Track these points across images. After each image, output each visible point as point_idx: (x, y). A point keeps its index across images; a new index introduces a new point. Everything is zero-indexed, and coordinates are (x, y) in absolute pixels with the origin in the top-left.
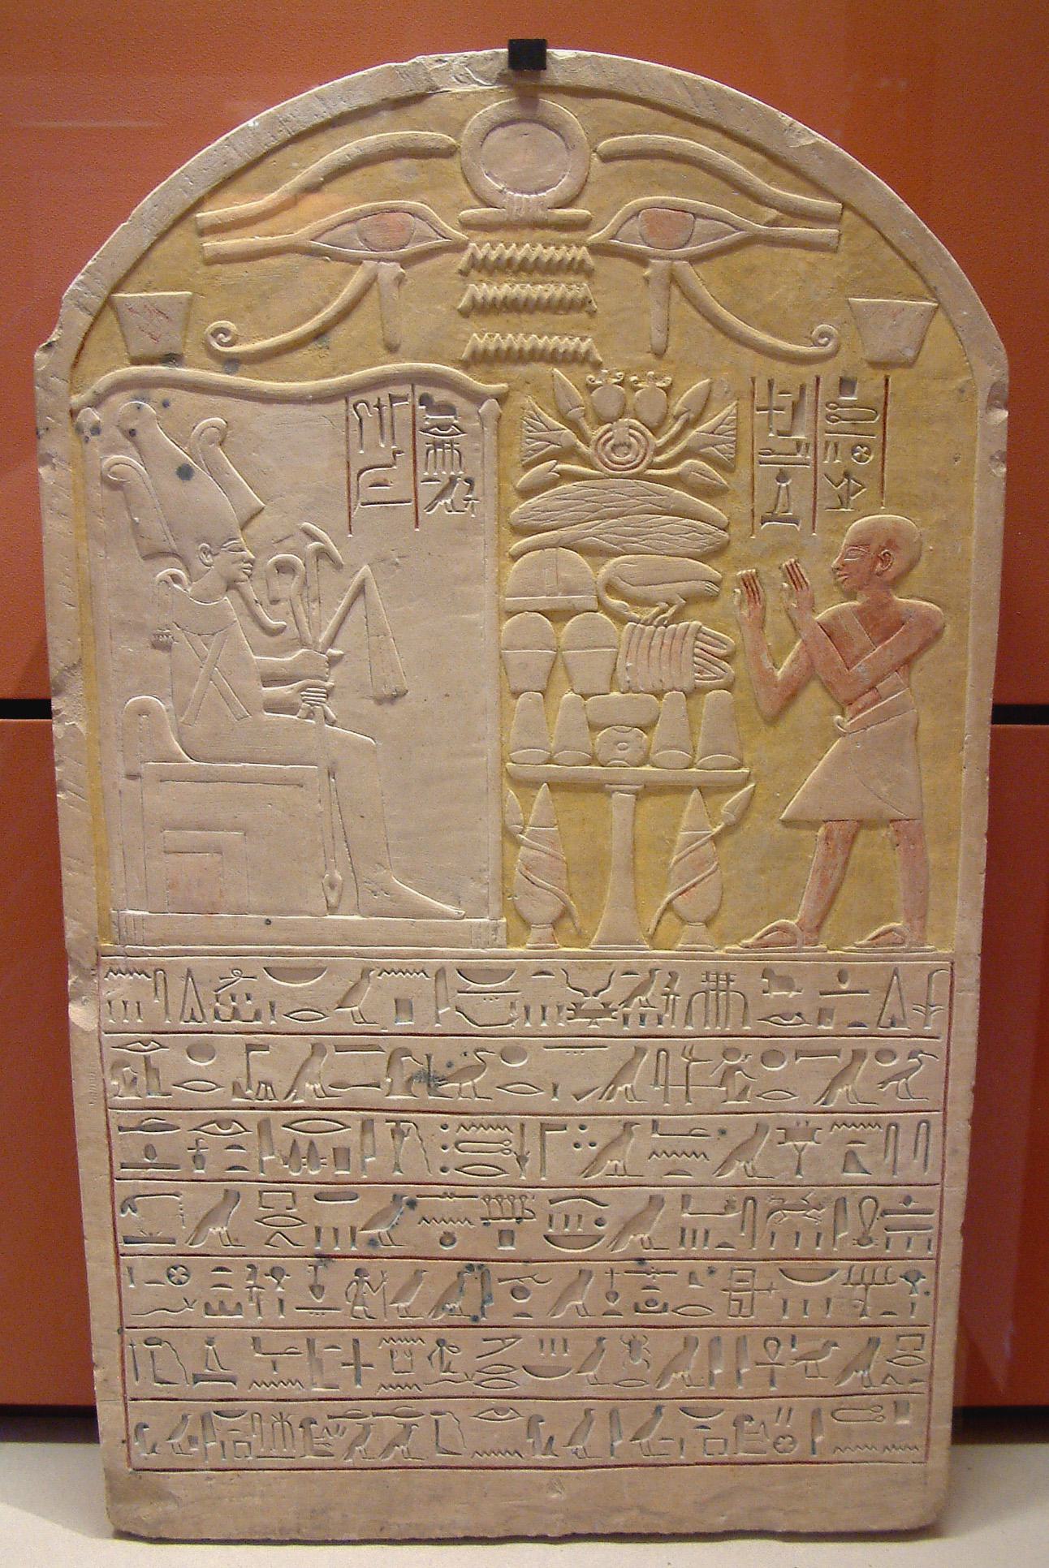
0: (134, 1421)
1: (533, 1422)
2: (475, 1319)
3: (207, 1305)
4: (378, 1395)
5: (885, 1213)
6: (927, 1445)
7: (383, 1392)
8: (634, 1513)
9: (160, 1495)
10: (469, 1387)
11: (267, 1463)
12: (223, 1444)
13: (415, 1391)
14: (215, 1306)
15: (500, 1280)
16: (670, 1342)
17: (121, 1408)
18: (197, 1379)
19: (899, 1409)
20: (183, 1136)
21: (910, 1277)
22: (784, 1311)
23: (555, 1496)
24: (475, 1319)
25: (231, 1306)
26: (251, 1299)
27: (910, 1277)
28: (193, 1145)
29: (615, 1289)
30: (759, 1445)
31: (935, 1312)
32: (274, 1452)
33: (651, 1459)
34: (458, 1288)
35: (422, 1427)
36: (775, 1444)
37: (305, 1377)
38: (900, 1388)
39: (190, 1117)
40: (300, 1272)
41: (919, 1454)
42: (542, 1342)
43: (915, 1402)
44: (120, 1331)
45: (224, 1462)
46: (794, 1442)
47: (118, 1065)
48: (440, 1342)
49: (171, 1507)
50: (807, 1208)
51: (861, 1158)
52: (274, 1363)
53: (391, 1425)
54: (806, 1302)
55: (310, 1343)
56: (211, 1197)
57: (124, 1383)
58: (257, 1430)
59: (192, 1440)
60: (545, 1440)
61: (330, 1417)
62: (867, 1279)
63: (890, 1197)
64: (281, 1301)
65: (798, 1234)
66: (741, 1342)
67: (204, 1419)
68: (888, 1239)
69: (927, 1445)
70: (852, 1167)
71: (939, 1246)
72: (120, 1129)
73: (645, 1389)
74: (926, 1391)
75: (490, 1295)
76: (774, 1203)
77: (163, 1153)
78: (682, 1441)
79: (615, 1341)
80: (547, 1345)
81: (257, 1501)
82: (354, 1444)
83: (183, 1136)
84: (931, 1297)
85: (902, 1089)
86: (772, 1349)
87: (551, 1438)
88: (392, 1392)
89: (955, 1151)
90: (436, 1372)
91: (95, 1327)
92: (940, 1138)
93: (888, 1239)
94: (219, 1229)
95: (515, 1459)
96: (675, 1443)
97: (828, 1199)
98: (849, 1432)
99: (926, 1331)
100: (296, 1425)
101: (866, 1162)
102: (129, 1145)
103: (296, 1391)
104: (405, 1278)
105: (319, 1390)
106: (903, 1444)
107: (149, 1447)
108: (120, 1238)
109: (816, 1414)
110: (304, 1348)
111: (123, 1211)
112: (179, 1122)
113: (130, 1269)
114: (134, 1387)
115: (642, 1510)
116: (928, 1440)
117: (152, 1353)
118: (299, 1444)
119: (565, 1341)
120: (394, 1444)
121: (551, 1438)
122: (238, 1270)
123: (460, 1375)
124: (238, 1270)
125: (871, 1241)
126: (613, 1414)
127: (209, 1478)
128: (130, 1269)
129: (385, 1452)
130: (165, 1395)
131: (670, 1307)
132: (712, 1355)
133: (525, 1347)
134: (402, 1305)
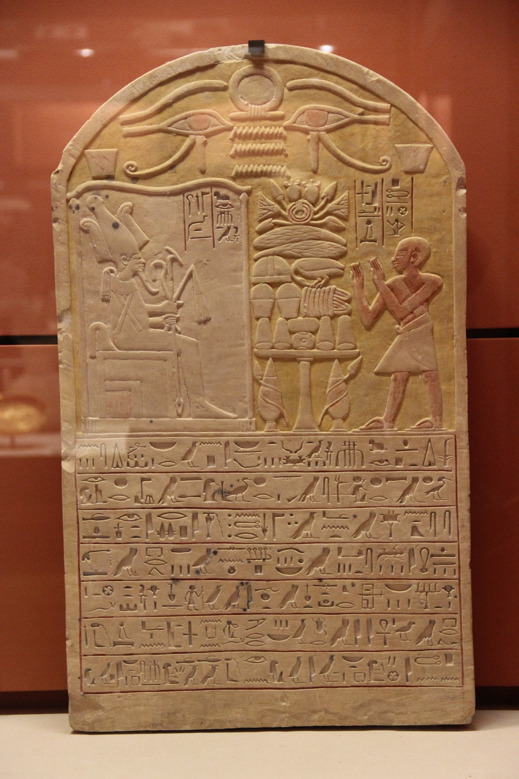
0: (84, 667)
1: (273, 664)
2: (245, 610)
3: (121, 606)
4: (200, 650)
5: (432, 556)
6: (463, 677)
7: (202, 649)
8: (323, 713)
9: (96, 707)
10: (242, 645)
11: (147, 688)
12: (126, 678)
13: (217, 648)
14: (125, 607)
15: (256, 590)
16: (335, 622)
17: (79, 661)
18: (115, 644)
19: (448, 658)
20: (112, 522)
21: (448, 588)
23: (284, 704)
24: (245, 610)
25: (132, 606)
26: (141, 602)
27: (448, 588)
28: (116, 526)
29: (309, 595)
30: (381, 676)
31: (460, 606)
32: (151, 682)
33: (329, 684)
34: (236, 595)
35: (221, 666)
36: (389, 676)
37: (165, 642)
38: (446, 646)
40: (164, 588)
41: (459, 682)
42: (276, 622)
43: (455, 654)
44: (80, 620)
45: (127, 688)
46: (397, 675)
48: (229, 623)
49: (101, 713)
50: (396, 553)
51: (420, 529)
52: (152, 635)
54: (398, 601)
55: (169, 624)
56: (124, 552)
58: (143, 669)
59: (112, 677)
60: (279, 674)
61: (178, 663)
62: (427, 589)
63: (435, 548)
64: (155, 603)
65: (392, 567)
66: (369, 622)
68: (435, 569)
69: (463, 677)
70: (416, 533)
73: (326, 646)
74: (460, 648)
75: (251, 598)
76: (380, 551)
78: (344, 674)
79: (310, 621)
81: (142, 708)
83: (112, 522)
84: (458, 598)
85: (436, 496)
86: (384, 625)
88: (207, 649)
89: (463, 526)
90: (226, 637)
91: (68, 618)
92: (456, 519)
93: (435, 569)
94: (127, 567)
95: (264, 684)
96: (340, 675)
97: (405, 549)
98: (424, 670)
99: (457, 616)
100: (161, 667)
101: (421, 530)
103: (162, 649)
104: (212, 590)
105: (172, 648)
106: (451, 676)
107: (91, 681)
108: (81, 573)
109: (407, 661)
110: (165, 627)
111: (83, 560)
112: (110, 515)
113: (86, 589)
114: (86, 648)
115: (327, 711)
116: (463, 674)
117: (94, 632)
118: (162, 677)
119: (287, 622)
120: (207, 677)
122: (135, 589)
123: (238, 639)
124: (135, 589)
125: (427, 571)
126: (311, 660)
127: (119, 697)
128: (86, 589)
129: (203, 681)
131: (335, 604)
132: (356, 630)
133: (268, 624)
134: (211, 603)
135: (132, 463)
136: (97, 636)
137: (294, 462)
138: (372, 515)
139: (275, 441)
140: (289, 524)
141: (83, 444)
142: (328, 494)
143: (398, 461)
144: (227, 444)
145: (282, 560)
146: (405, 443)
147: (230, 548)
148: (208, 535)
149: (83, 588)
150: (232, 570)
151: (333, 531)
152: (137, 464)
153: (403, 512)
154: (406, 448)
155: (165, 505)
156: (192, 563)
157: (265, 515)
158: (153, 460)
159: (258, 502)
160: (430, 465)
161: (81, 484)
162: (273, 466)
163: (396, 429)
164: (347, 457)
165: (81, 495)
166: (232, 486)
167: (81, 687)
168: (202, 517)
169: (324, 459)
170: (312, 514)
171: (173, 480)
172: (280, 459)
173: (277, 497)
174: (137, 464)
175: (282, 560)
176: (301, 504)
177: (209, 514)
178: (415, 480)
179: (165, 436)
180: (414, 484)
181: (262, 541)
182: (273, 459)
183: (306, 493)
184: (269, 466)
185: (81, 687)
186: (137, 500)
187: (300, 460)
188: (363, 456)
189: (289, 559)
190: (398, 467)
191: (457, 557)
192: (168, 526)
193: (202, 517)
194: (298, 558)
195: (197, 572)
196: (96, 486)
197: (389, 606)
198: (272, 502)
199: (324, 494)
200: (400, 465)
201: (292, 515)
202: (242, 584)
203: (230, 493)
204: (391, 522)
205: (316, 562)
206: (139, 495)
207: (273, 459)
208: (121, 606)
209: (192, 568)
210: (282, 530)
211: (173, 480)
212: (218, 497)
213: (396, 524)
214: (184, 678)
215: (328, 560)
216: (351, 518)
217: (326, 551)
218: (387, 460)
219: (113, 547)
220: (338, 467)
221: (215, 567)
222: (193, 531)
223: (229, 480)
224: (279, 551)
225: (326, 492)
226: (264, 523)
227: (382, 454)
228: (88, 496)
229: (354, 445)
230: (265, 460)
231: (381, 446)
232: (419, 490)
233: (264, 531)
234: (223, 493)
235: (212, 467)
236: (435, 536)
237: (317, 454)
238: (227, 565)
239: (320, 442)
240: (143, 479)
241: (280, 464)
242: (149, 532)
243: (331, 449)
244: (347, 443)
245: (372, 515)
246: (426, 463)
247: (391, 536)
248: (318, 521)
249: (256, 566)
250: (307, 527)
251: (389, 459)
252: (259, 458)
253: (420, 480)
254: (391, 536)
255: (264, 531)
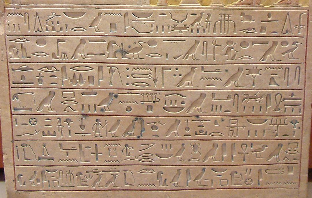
1: (159, 174)
2: (139, 137)
3: (43, 132)
4: (104, 164)
5: (284, 99)
6: (299, 182)
7: (106, 163)
10: (136, 161)
11: (65, 188)
12: (49, 182)
13: (117, 163)
14: (46, 132)
15: (148, 123)
16: (208, 145)
17: (13, 169)
19: (289, 169)
20: (35, 72)
22: (248, 134)
24: (139, 137)
25: (52, 133)
26: (59, 130)
28: (38, 75)
29: (188, 126)
30: (239, 182)
31: (302, 135)
32: (67, 185)
33: (201, 187)
34: (133, 126)
35: (120, 176)
36: (245, 182)
37: (78, 158)
38: (289, 161)
39: (37, 65)
40: (76, 121)
41: (296, 185)
42: (162, 145)
43: (295, 166)
44: (12, 141)
46: (252, 181)
47: (11, 47)
50: (256, 98)
52: (67, 153)
53: (109, 175)
54: (256, 131)
55: (80, 146)
56: (45, 94)
57: (14, 160)
58: (61, 177)
59: (38, 180)
61: (87, 172)
62: (278, 123)
64: (70, 131)
65: (253, 107)
66: (233, 145)
67: (42, 173)
68: (285, 109)
69: (299, 182)
70: (273, 83)
71: (303, 112)
72: (12, 69)
73: (199, 162)
74: (299, 163)
75: (144, 129)
76: (245, 96)
77: (28, 78)
78: (212, 181)
79: (188, 145)
80: (164, 146)
82: (96, 181)
83: (35, 72)
84: (301, 129)
86: (244, 148)
87: (166, 180)
91: (3, 140)
92: (304, 73)
93: (285, 109)
94: (47, 105)
95: (153, 187)
96: (210, 181)
98: (271, 177)
100: (75, 175)
101: (278, 81)
102: (16, 75)
103: (75, 163)
104: (113, 122)
105: (83, 162)
106: (291, 181)
107: (23, 183)
108: (12, 108)
109: (260, 171)
110: (78, 148)
111: (13, 99)
112: (33, 67)
113: (16, 119)
116: (300, 180)
117: (24, 149)
118: (76, 182)
119: (171, 145)
120: (110, 182)
121: (166, 180)
123: (133, 157)
125: (279, 109)
126: (188, 171)
127: (44, 194)
128: (16, 119)
129: (107, 184)
130: (28, 164)
131: (208, 133)
132: (223, 150)
133: (156, 148)
134: (113, 132)
135: (50, 28)
136: (25, 153)
137: (180, 29)
138: (240, 70)
139: (165, 13)
140: (175, 75)
141: (11, 12)
142: (206, 54)
143: (262, 29)
144: (126, 14)
145: (168, 102)
146: (269, 15)
147: (128, 93)
148: (111, 83)
149: (14, 119)
150: (129, 109)
151: (209, 81)
152: (53, 29)
153: (264, 68)
154: (270, 19)
155: (76, 60)
156: (98, 104)
157: (155, 68)
158: (66, 26)
159: (151, 59)
160: (287, 32)
161: (9, 43)
162: (163, 32)
163: (263, 5)
164: (223, 26)
165: (10, 51)
166: (129, 47)
167: (16, 186)
168: (106, 70)
169: (204, 27)
170: (193, 68)
171: (82, 41)
172: (169, 27)
173: (166, 55)
174: (53, 29)
175: (168, 102)
176: (184, 61)
177: (111, 67)
178: (275, 43)
179: (75, 7)
180: (274, 47)
181: (153, 88)
182: (163, 27)
183: (188, 53)
184: (160, 32)
185: (16, 186)
186: (54, 55)
187: (185, 27)
188: (235, 25)
189: (173, 102)
190: (262, 33)
191: (302, 100)
192: (79, 76)
193: (106, 70)
194: (181, 101)
195: (102, 110)
196: (22, 45)
197: (249, 134)
198: (162, 59)
199: (203, 53)
200: (264, 32)
201: (177, 69)
202: (137, 119)
203: (128, 52)
204: (254, 75)
205: (193, 104)
206: (56, 52)
207: (163, 27)
208: (43, 132)
209: (98, 107)
210: (169, 80)
211: (82, 41)
212: (119, 55)
213: (258, 76)
214: (92, 182)
215: (204, 102)
216: (224, 72)
217: (203, 95)
218: (254, 29)
219: (36, 91)
220: (215, 34)
221: (117, 106)
222: (99, 80)
223: (127, 42)
224: (166, 96)
225: (205, 52)
226: (155, 75)
227: (250, 24)
228: (15, 52)
229: (229, 17)
230: (157, 27)
231: (249, 18)
232: (277, 52)
233: (155, 80)
234: (123, 52)
235: (113, 32)
236: (287, 85)
237: (198, 23)
238: (125, 105)
239: (201, 14)
240: (58, 41)
241: (169, 31)
242: (64, 80)
243: (210, 19)
244: (223, 15)
245: (240, 70)
246: (284, 31)
247: (253, 85)
248: (198, 74)
249: (148, 106)
250: (188, 78)
251: (256, 27)
252: (152, 26)
253: (279, 43)
254: (253, 85)
255: (155, 80)
